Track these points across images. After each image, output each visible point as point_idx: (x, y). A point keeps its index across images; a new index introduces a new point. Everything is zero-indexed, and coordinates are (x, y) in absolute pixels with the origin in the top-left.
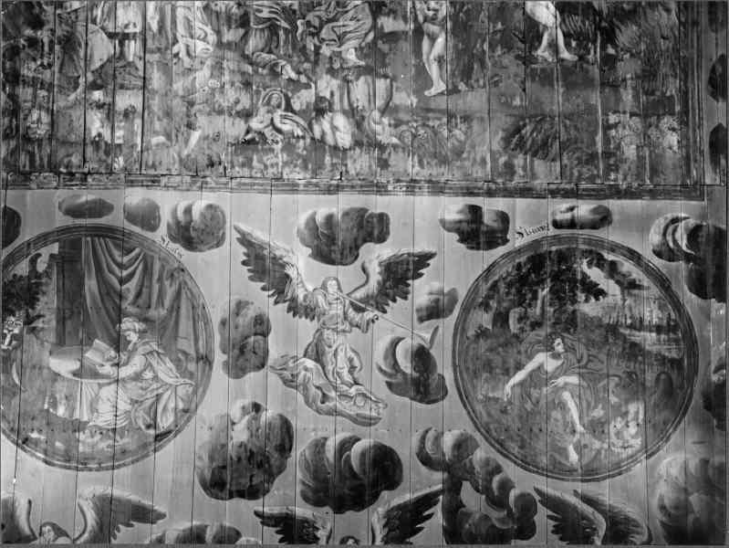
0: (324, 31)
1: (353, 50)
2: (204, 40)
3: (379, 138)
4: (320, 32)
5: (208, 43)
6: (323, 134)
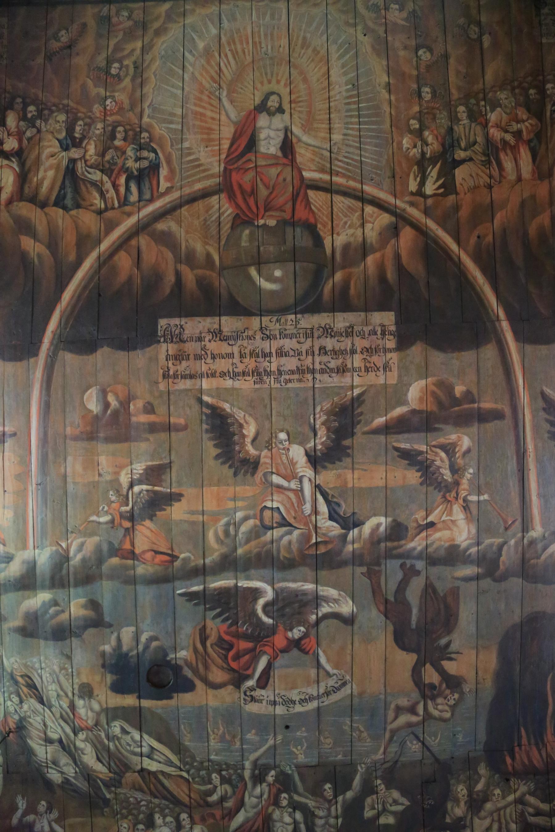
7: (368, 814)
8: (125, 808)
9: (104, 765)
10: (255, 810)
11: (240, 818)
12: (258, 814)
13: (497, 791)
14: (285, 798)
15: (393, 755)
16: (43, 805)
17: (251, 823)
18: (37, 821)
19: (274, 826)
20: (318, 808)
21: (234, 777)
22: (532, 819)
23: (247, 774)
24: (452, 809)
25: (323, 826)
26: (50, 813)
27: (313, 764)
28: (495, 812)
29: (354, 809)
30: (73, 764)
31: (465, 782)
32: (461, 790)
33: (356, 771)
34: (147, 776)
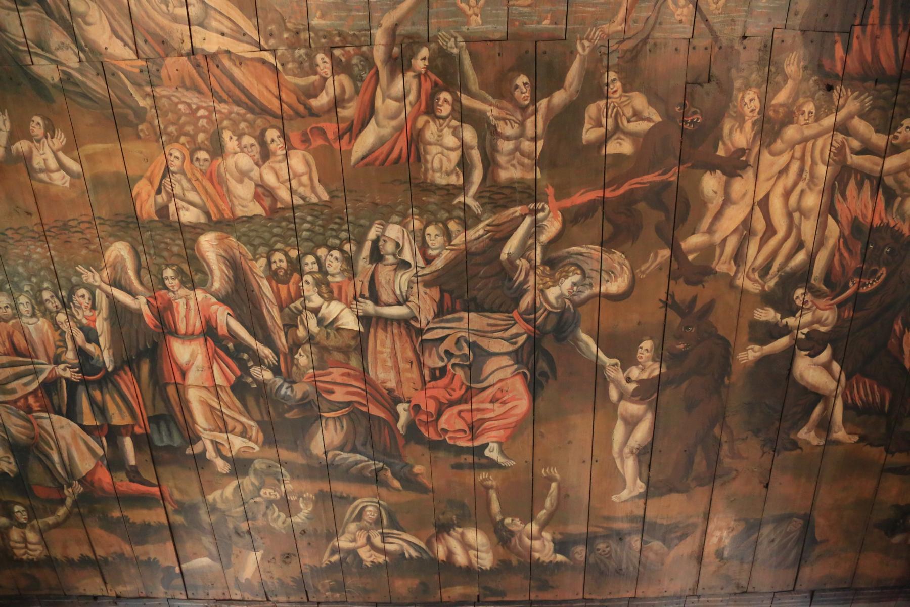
0: (444, 418)
1: (496, 446)
2: (244, 434)
3: (536, 555)
4: (438, 419)
5: (250, 439)
6: (450, 554)
7: (590, 134)
8: (173, 124)
9: (126, 44)
10: (394, 123)
11: (368, 138)
12: (399, 130)
13: (810, 107)
14: (446, 100)
15: (640, 25)
16: (37, 125)
17: (386, 148)
18: (35, 152)
19: (426, 152)
20: (504, 120)
21: (355, 61)
22: (854, 160)
23: (379, 54)
24: (730, 132)
25: (512, 153)
26: (52, 137)
27: (497, 36)
28: (799, 143)
29: (565, 123)
30: (74, 46)
31: (758, 86)
32: (750, 101)
33: (573, 53)
34: (203, 63)
